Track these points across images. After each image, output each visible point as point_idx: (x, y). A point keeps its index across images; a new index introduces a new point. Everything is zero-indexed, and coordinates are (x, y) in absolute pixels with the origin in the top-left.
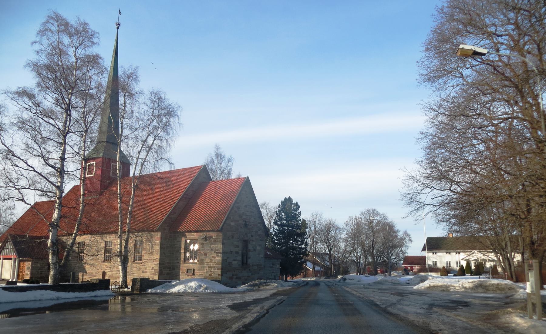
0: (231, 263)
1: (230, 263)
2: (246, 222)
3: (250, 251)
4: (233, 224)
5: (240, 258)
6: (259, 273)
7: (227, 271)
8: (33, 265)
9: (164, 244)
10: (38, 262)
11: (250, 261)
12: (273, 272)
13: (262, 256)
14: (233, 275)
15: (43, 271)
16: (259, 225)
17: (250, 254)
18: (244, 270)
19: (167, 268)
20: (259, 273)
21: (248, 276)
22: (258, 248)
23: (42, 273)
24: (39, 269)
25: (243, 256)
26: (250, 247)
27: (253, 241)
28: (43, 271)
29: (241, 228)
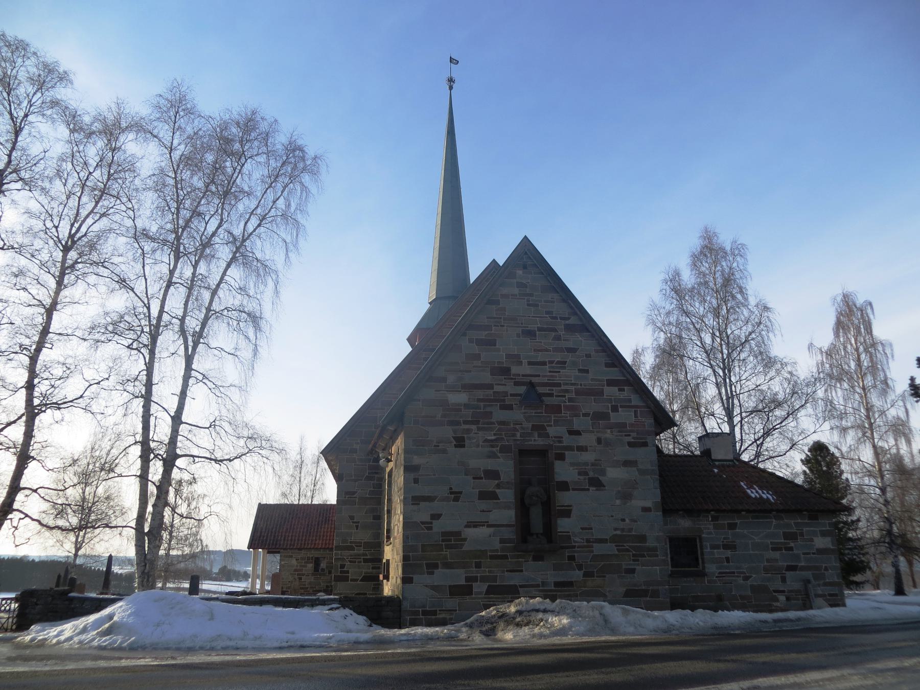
1: (453, 538)
2: (532, 385)
3: (564, 486)
5: (509, 515)
6: (633, 571)
7: (432, 567)
8: (283, 563)
9: (354, 493)
10: (291, 557)
11: (563, 525)
13: (648, 504)
14: (468, 579)
15: (303, 575)
17: (563, 498)
18: (537, 558)
19: (366, 561)
20: (633, 571)
22: (614, 474)
23: (300, 579)
24: (296, 570)
25: (523, 508)
26: (564, 471)
27: (581, 449)
28: (303, 575)
29: (506, 407)
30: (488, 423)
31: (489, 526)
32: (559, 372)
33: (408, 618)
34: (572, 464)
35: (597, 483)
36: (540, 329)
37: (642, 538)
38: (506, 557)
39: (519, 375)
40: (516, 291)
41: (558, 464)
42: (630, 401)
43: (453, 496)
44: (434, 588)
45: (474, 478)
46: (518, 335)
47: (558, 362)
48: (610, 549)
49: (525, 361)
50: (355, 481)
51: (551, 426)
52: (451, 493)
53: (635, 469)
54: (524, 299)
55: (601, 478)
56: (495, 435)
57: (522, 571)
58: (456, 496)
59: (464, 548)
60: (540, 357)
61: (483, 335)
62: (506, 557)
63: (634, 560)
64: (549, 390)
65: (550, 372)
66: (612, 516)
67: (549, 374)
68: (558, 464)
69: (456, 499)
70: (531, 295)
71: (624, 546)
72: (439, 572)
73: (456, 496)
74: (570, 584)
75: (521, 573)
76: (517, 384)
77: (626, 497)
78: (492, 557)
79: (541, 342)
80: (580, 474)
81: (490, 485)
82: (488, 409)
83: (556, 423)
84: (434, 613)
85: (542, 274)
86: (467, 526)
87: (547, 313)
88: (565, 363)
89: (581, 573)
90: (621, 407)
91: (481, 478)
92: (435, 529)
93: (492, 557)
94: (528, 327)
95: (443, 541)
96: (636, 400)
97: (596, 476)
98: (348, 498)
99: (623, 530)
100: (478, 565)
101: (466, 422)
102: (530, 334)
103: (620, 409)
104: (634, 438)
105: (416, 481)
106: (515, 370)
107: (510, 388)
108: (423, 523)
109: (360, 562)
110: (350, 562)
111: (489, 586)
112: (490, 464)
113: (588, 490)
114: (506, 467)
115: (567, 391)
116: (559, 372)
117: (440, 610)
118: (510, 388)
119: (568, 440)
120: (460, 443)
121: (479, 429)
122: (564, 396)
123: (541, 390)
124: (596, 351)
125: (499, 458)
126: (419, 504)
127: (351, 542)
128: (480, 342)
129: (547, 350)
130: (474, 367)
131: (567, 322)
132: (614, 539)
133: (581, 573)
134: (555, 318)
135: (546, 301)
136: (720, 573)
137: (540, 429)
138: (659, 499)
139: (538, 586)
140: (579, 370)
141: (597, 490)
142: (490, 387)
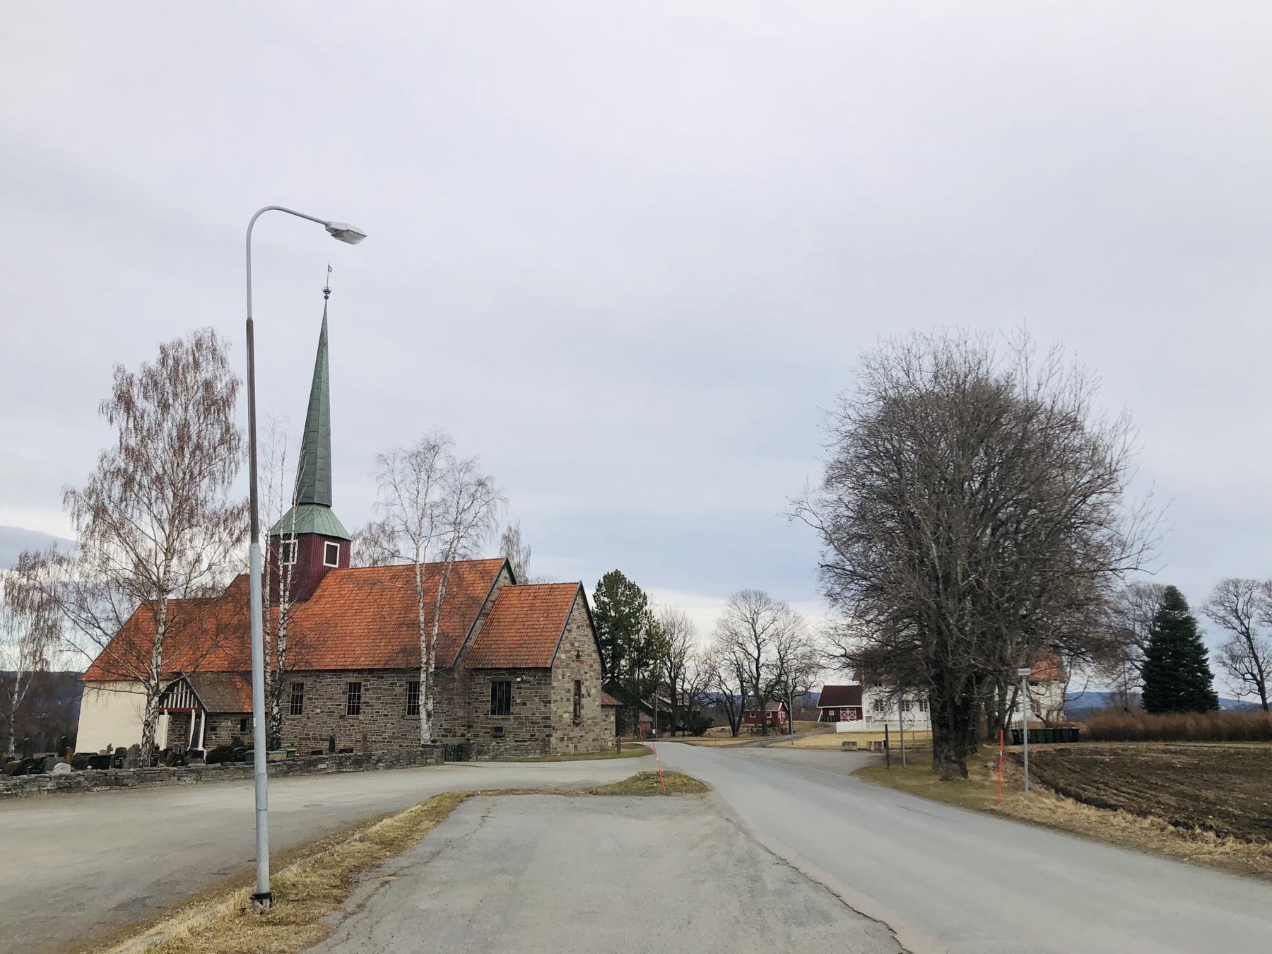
0: (562, 716)
4: (563, 656)
5: (571, 709)
10: (228, 719)
12: (606, 729)
14: (564, 735)
17: (584, 701)
21: (581, 736)
22: (593, 691)
24: (230, 731)
26: (583, 691)
27: (587, 680)
29: (573, 661)
36: (581, 626)
37: (596, 718)
70: (579, 609)
76: (576, 650)
77: (594, 701)
84: (556, 749)
102: (578, 627)
114: (571, 686)
142: (569, 651)
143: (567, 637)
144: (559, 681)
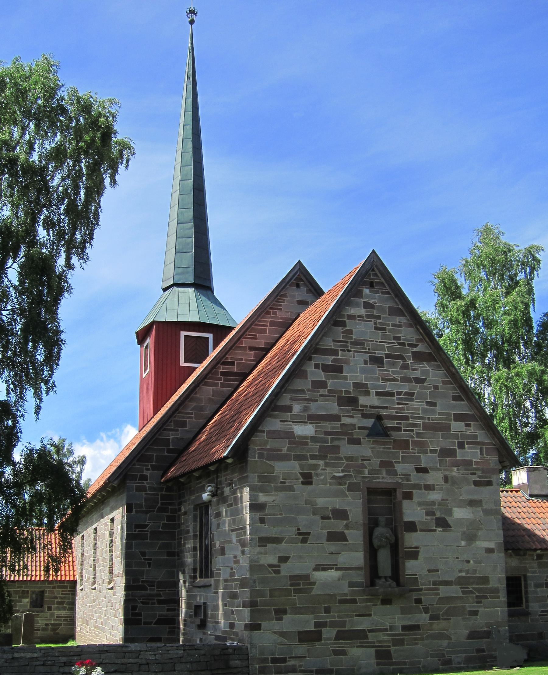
0: (307, 577)
2: (379, 418)
3: (411, 527)
6: (475, 613)
7: (280, 613)
9: (146, 526)
13: (491, 545)
14: (317, 625)
16: (457, 426)
18: (386, 601)
19: (160, 602)
20: (475, 613)
27: (429, 488)
30: (335, 459)
31: (338, 569)
32: (407, 404)
33: (257, 666)
34: (420, 504)
35: (443, 523)
36: (388, 356)
37: (485, 580)
38: (354, 601)
39: (366, 406)
40: (363, 312)
41: (406, 503)
42: (476, 437)
43: (301, 537)
44: (282, 634)
45: (323, 518)
46: (365, 362)
47: (406, 394)
48: (455, 591)
49: (373, 391)
50: (146, 512)
51: (399, 462)
52: (300, 534)
53: (479, 509)
54: (371, 321)
55: (447, 518)
56: (343, 471)
57: (370, 615)
58: (304, 537)
59: (314, 592)
60: (389, 387)
61: (329, 360)
62: (354, 601)
63: (477, 602)
64: (398, 424)
65: (398, 404)
66: (458, 558)
67: (397, 406)
68: (406, 503)
69: (304, 541)
70: (379, 317)
71: (469, 588)
72: (287, 618)
73: (304, 537)
74: (416, 627)
75: (370, 618)
76: (365, 416)
77: (471, 538)
78: (342, 602)
79: (389, 371)
80: (427, 514)
81: (338, 526)
82: (336, 443)
83: (405, 460)
84: (284, 660)
85: (388, 293)
86: (315, 570)
87: (395, 338)
88: (413, 394)
89: (427, 616)
90: (468, 443)
91: (329, 518)
92: (283, 573)
93: (342, 602)
94: (375, 353)
95: (291, 585)
96: (482, 436)
97: (443, 516)
98: (138, 531)
99: (467, 572)
100: (327, 610)
101: (313, 457)
102: (377, 361)
103: (466, 446)
104: (479, 477)
105: (262, 521)
106: (362, 400)
107: (356, 420)
108: (270, 566)
109: (154, 603)
110: (143, 603)
111: (338, 631)
112: (337, 503)
113: (435, 530)
115: (415, 425)
116: (407, 404)
117: (289, 658)
118: (356, 420)
119: (415, 478)
120: (307, 480)
121: (327, 465)
122: (412, 431)
123: (389, 423)
124: (444, 382)
125: (347, 496)
126: (266, 546)
127: (143, 582)
128: (326, 368)
129: (395, 380)
130: (321, 395)
131: (415, 349)
132: (462, 581)
133: (427, 616)
134: (404, 344)
135: (394, 325)
136: (542, 611)
137: (387, 465)
138: (501, 540)
139: (386, 630)
140: (427, 403)
141: (443, 531)
142: (337, 418)
143: (319, 385)
144: (284, 488)
